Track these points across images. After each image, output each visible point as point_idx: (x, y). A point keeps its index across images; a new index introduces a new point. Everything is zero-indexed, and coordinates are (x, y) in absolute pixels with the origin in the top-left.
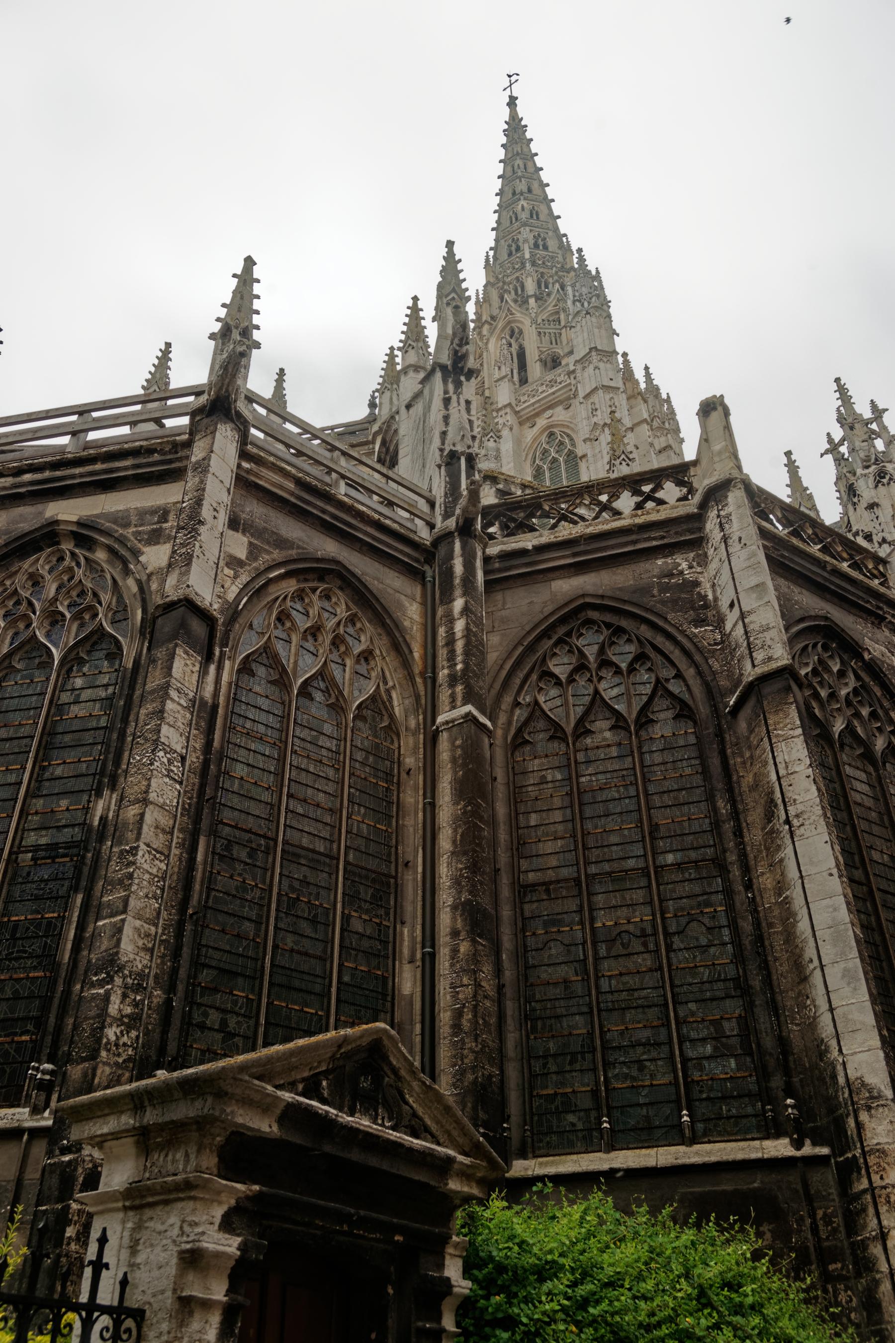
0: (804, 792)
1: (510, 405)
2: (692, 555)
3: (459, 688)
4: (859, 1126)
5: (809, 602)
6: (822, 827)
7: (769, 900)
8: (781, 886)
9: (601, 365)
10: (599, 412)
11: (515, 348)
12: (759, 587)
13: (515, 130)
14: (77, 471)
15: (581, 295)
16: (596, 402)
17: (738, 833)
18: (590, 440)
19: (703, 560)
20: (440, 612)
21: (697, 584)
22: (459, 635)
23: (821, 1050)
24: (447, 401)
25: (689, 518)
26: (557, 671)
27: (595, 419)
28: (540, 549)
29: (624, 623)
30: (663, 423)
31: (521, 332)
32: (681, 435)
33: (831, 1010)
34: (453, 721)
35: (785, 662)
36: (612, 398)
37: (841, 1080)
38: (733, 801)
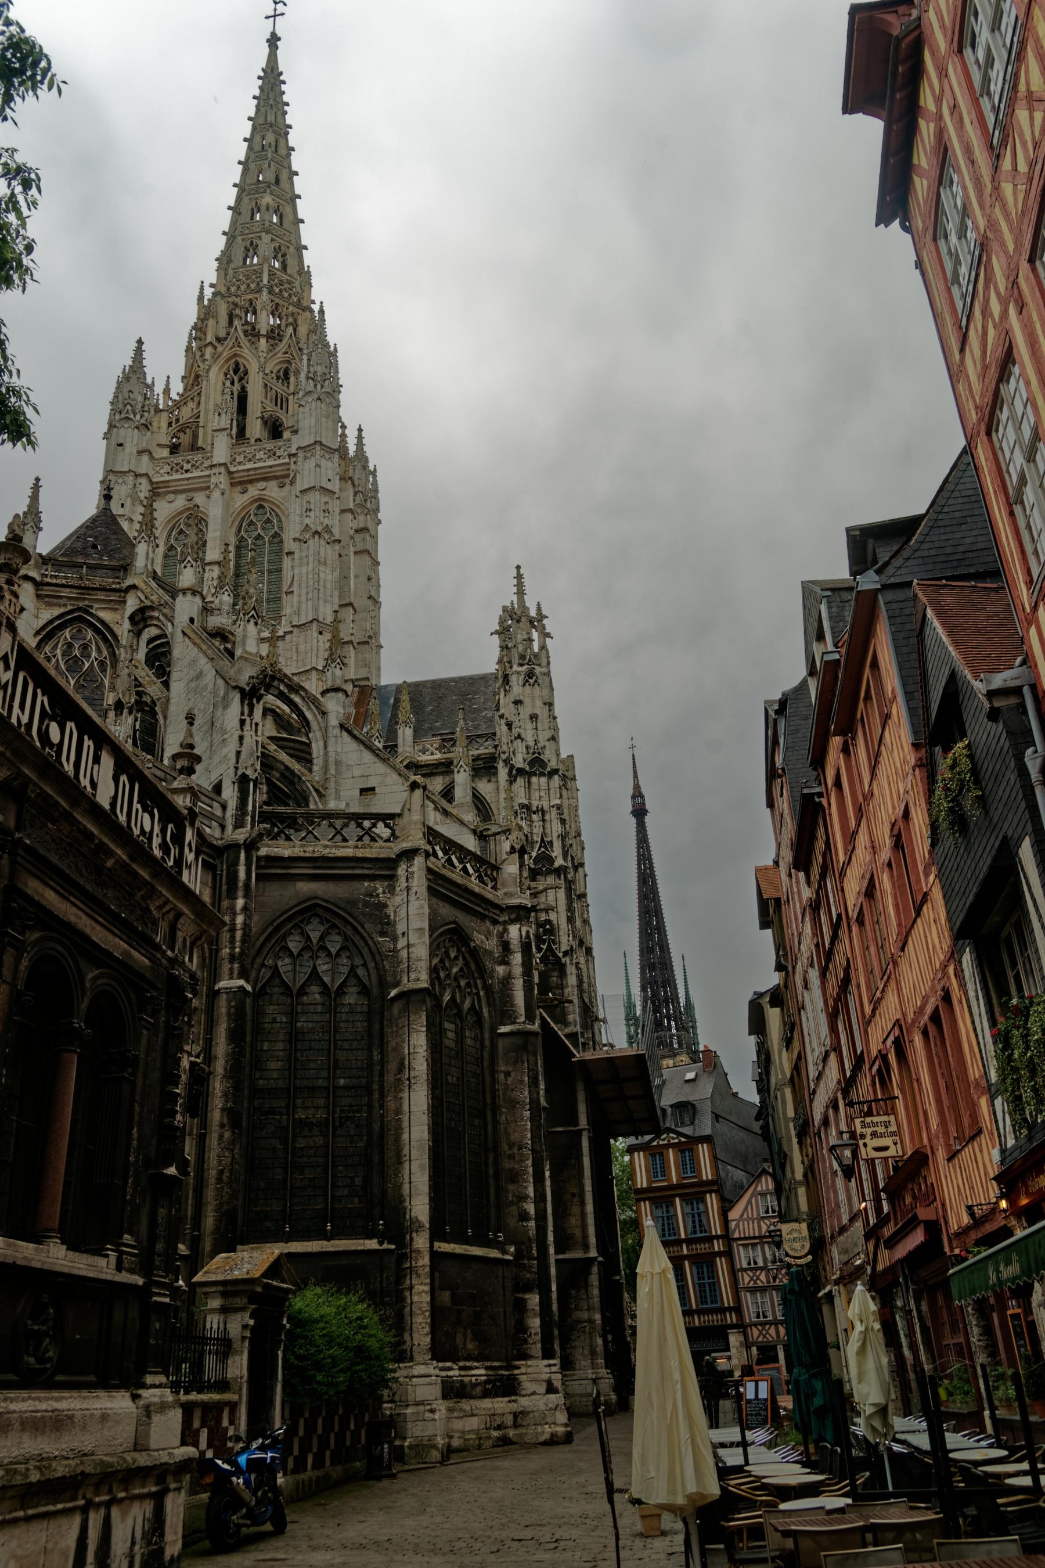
0: (420, 1066)
1: (225, 464)
2: (386, 883)
3: (236, 966)
4: (412, 1239)
5: (446, 911)
6: (425, 1087)
9: (323, 462)
10: (312, 514)
11: (237, 387)
13: (271, 81)
15: (315, 372)
16: (312, 501)
17: (382, 1075)
18: (300, 540)
19: (392, 890)
20: (225, 903)
21: (385, 906)
22: (239, 926)
23: (401, 1199)
24: (242, 722)
25: (388, 860)
26: (291, 945)
27: (307, 521)
28: (291, 859)
29: (337, 921)
30: (366, 501)
31: (246, 373)
32: (380, 516)
33: (410, 1183)
34: (231, 988)
35: (425, 985)
36: (326, 503)
37: (408, 1217)
38: (382, 1053)
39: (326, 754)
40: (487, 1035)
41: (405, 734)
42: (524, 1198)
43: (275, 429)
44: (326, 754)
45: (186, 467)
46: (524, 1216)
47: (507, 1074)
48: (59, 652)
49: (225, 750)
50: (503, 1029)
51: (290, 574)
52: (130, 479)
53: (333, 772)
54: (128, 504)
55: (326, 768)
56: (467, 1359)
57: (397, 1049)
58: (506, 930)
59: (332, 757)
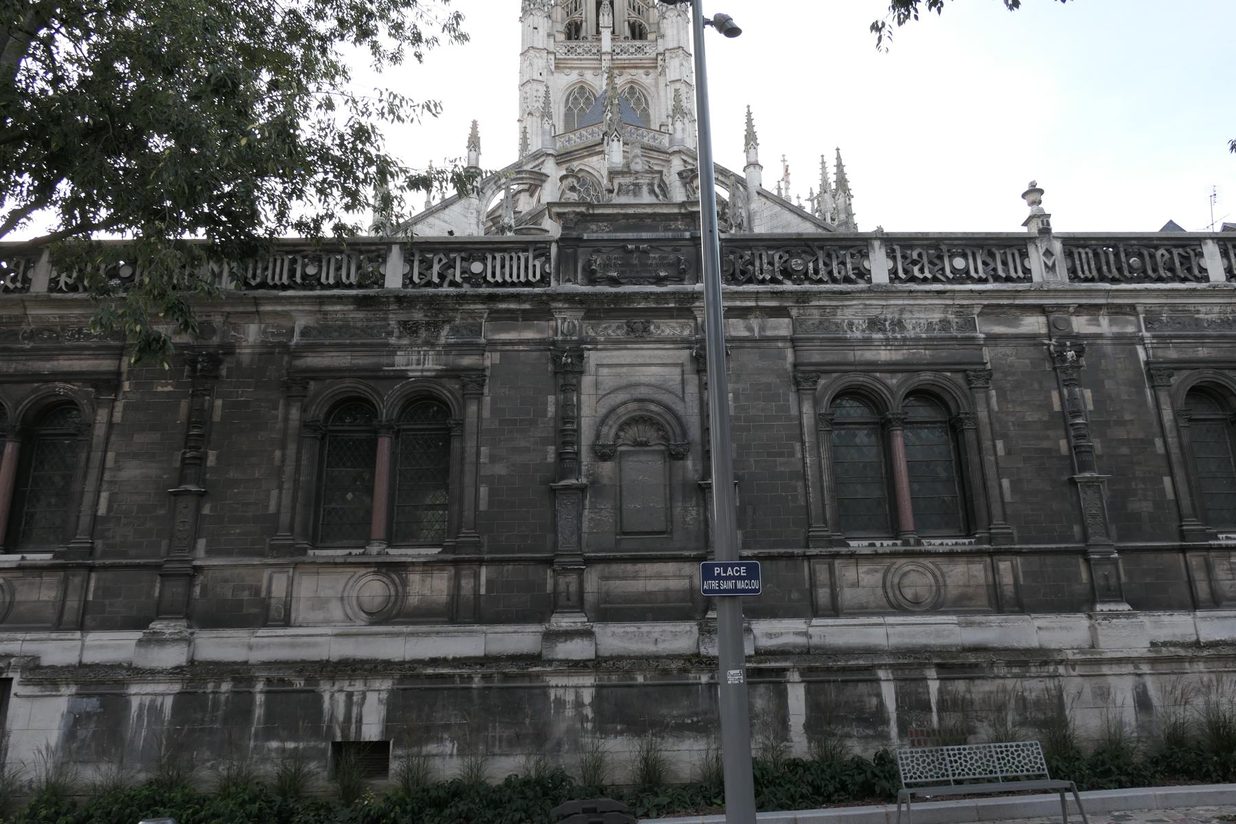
43: (637, 32)
45: (579, 51)
52: (544, 54)
54: (544, 74)
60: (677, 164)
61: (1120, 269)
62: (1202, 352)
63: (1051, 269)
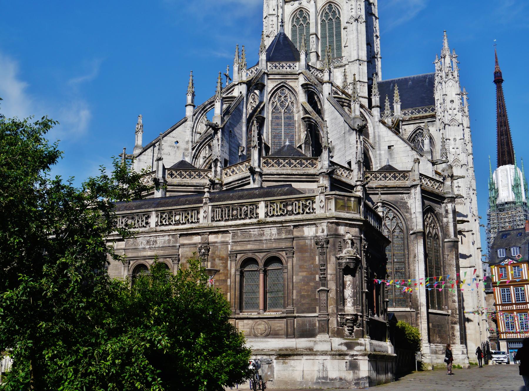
0: (421, 256)
7: (412, 271)
8: (414, 270)
12: (419, 212)
14: (293, 177)
17: (408, 258)
19: (409, 197)
21: (407, 203)
24: (357, 141)
39: (374, 132)
40: (441, 242)
41: (397, 107)
42: (454, 296)
44: (374, 132)
46: (454, 301)
47: (448, 255)
48: (276, 99)
49: (351, 151)
50: (446, 240)
51: (346, 38)
53: (377, 139)
55: (375, 137)
56: (438, 343)
57: (413, 250)
58: (446, 205)
59: (377, 134)
60: (302, 80)
61: (229, 216)
62: (249, 247)
63: (205, 218)
